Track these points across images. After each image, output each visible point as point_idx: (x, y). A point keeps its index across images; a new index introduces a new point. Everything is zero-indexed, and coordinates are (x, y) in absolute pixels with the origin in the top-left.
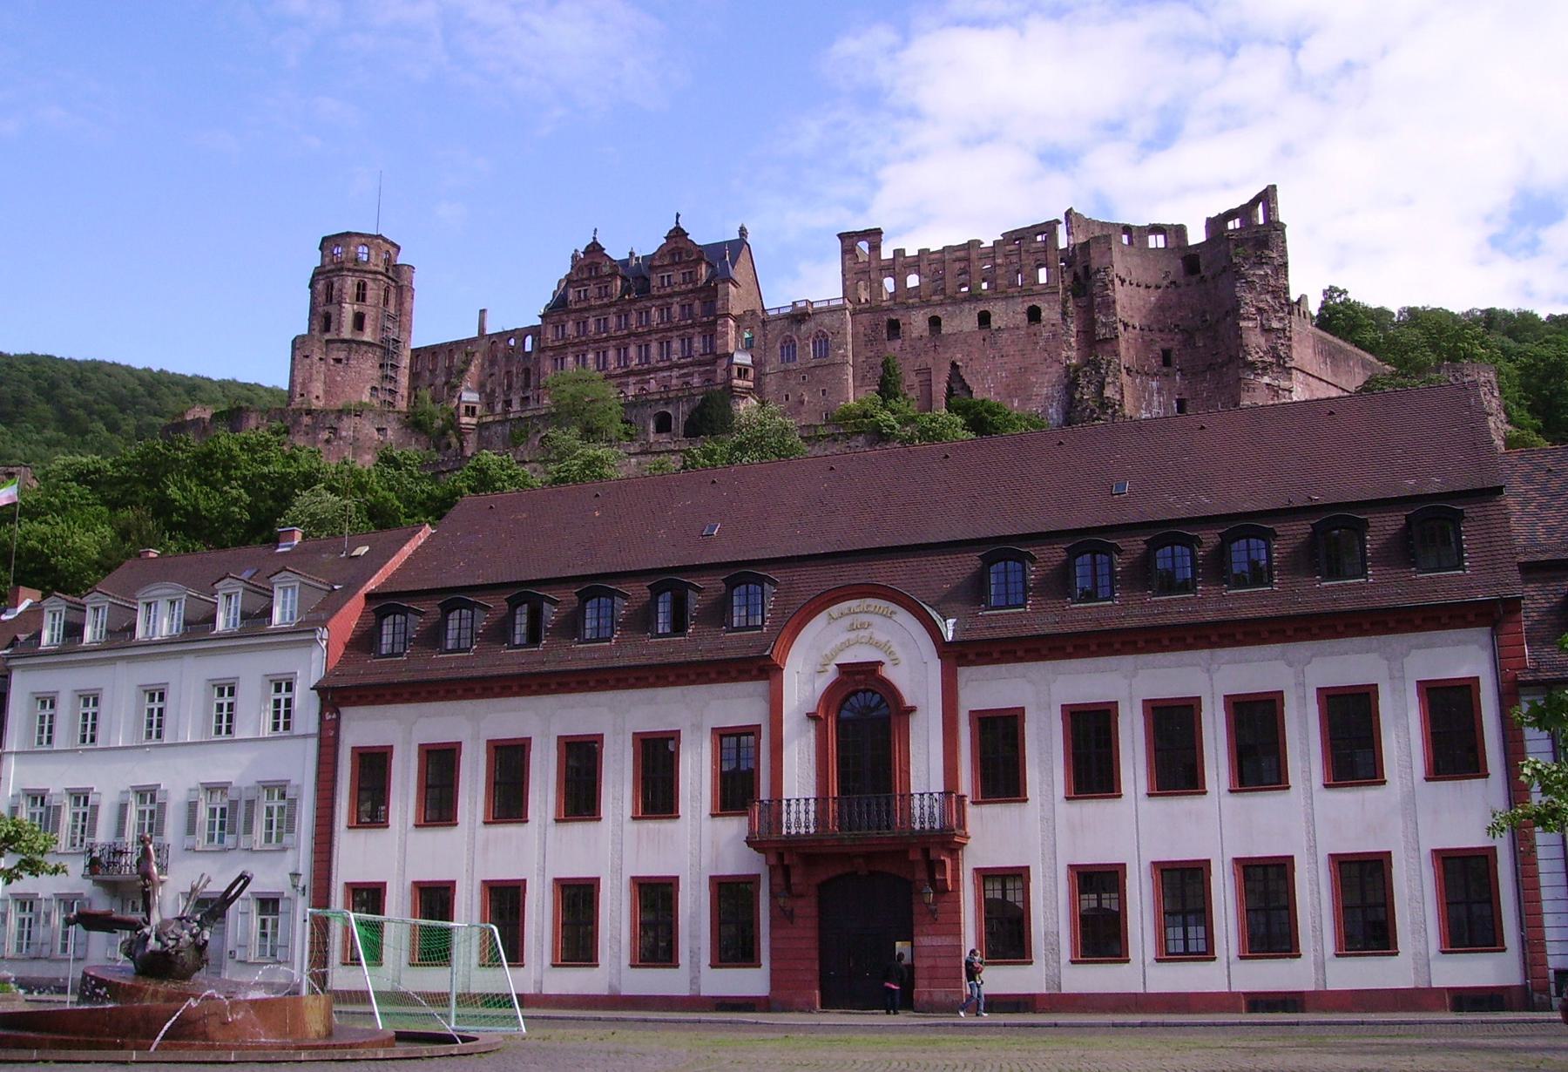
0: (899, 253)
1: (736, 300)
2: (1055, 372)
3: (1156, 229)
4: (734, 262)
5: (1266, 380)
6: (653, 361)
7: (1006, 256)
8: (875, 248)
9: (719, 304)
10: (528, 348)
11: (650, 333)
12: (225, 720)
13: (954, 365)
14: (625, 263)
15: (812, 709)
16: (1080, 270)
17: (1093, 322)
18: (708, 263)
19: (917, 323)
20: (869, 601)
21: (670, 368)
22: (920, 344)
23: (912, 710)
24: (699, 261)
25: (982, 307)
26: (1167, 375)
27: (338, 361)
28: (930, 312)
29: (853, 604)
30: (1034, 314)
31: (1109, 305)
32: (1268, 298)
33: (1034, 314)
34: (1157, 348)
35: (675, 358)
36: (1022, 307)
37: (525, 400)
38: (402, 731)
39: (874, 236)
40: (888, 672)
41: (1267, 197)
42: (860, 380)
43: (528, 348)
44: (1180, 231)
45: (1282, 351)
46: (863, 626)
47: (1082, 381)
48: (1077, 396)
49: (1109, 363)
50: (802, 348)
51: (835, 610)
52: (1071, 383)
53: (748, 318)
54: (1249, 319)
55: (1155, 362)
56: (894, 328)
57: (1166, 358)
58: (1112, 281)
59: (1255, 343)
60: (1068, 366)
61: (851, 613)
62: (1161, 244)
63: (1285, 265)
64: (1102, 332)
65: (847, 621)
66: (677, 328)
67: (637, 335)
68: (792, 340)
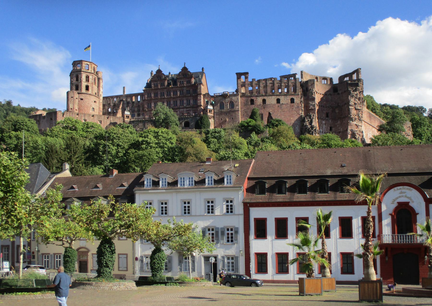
0: (253, 80)
1: (203, 90)
2: (299, 116)
3: (325, 78)
4: (202, 77)
5: (355, 123)
6: (178, 106)
7: (285, 83)
8: (246, 78)
9: (198, 90)
10: (139, 100)
11: (177, 97)
12: (210, 210)
13: (270, 114)
14: (168, 76)
15: (391, 213)
16: (305, 89)
17: (309, 103)
18: (194, 78)
19: (259, 100)
20: (405, 187)
21: (183, 108)
22: (260, 107)
23: (418, 214)
24: (191, 77)
25: (278, 97)
26: (327, 120)
27: (82, 99)
28: (263, 98)
29: (401, 187)
30: (292, 101)
31: (313, 99)
32: (357, 100)
33: (292, 101)
34: (325, 112)
35: (185, 105)
36: (289, 98)
37: (139, 115)
38: (271, 215)
39: (246, 74)
40: (411, 204)
41: (357, 71)
42: (243, 116)
43: (139, 100)
44: (331, 79)
45: (360, 115)
46: (405, 193)
47: (306, 120)
48: (305, 124)
49: (313, 115)
50: (226, 105)
51: (396, 188)
52: (302, 120)
53: (207, 95)
54: (352, 106)
55: (324, 116)
56: (252, 102)
57: (327, 116)
58: (314, 93)
59: (353, 112)
60: (302, 116)
61: (400, 189)
62: (326, 83)
63: (363, 92)
64: (311, 107)
65: (399, 191)
66: (186, 97)
67: (174, 98)
68: (223, 103)
